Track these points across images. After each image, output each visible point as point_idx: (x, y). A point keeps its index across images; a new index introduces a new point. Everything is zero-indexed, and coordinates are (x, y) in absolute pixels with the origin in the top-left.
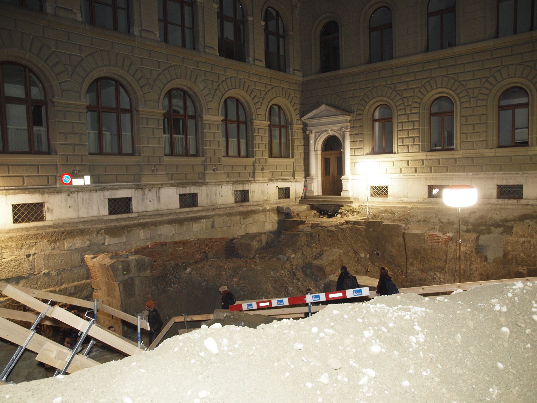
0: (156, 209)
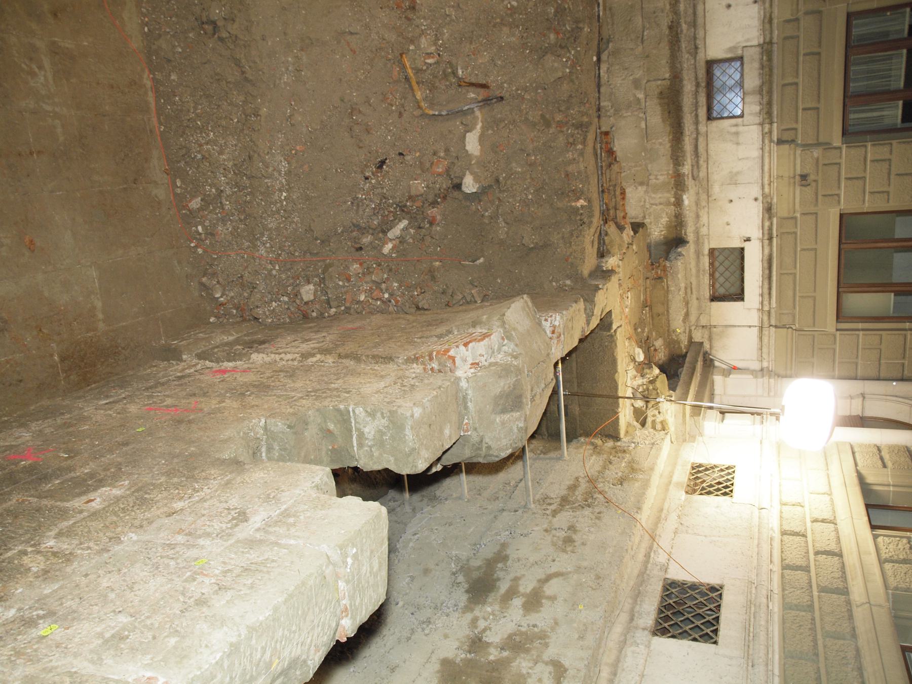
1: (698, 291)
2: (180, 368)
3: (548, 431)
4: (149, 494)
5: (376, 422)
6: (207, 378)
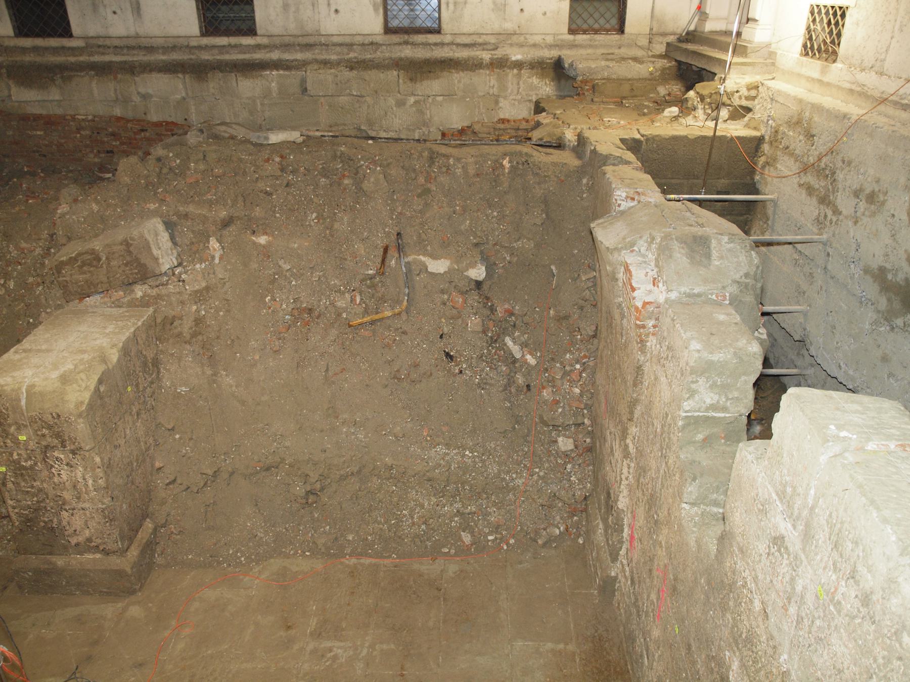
0: (132, 32)
1: (611, 47)
2: (623, 580)
3: (742, 215)
4: (742, 633)
5: (702, 390)
6: (636, 556)
